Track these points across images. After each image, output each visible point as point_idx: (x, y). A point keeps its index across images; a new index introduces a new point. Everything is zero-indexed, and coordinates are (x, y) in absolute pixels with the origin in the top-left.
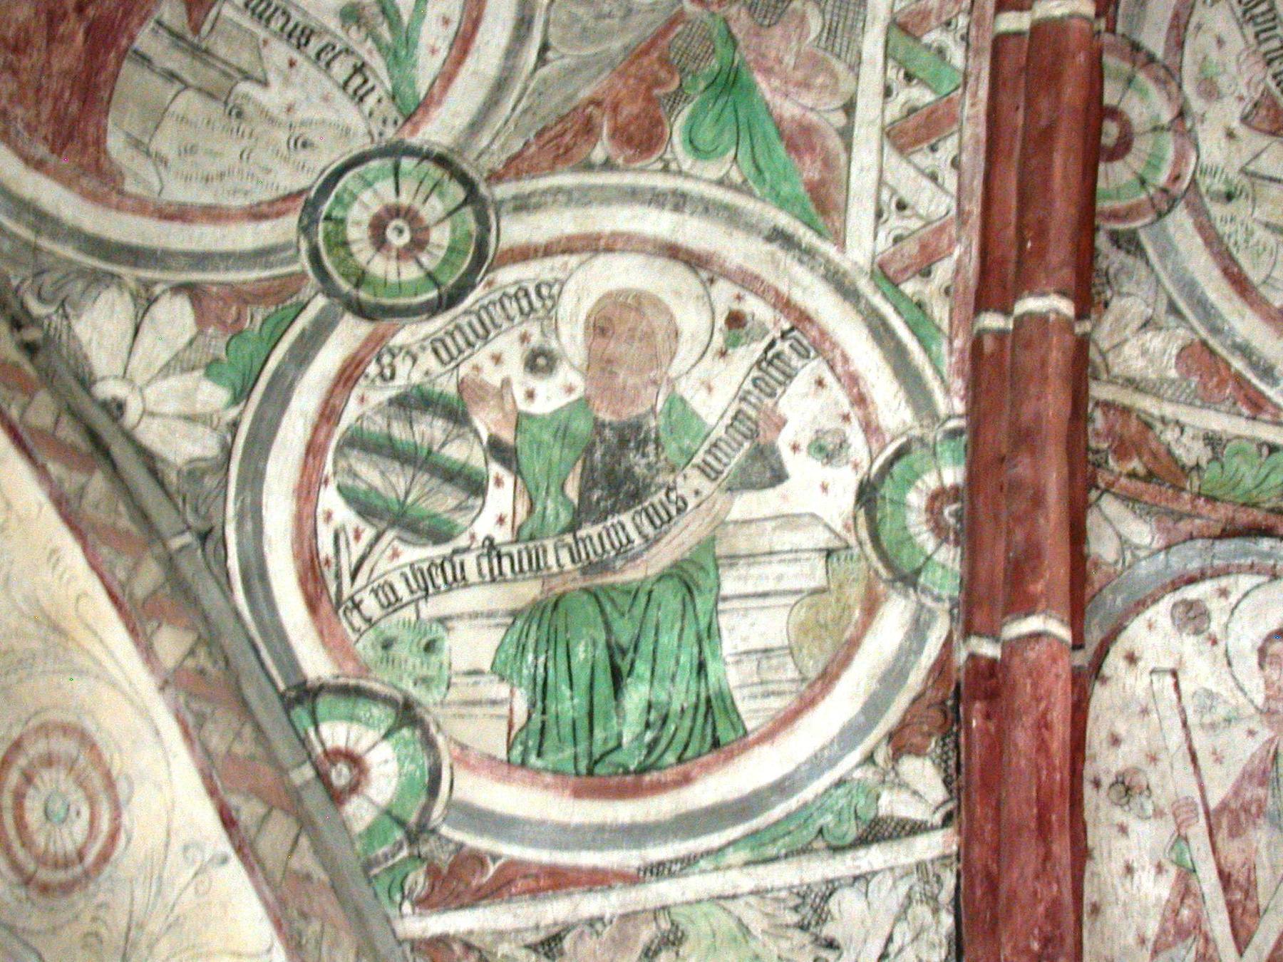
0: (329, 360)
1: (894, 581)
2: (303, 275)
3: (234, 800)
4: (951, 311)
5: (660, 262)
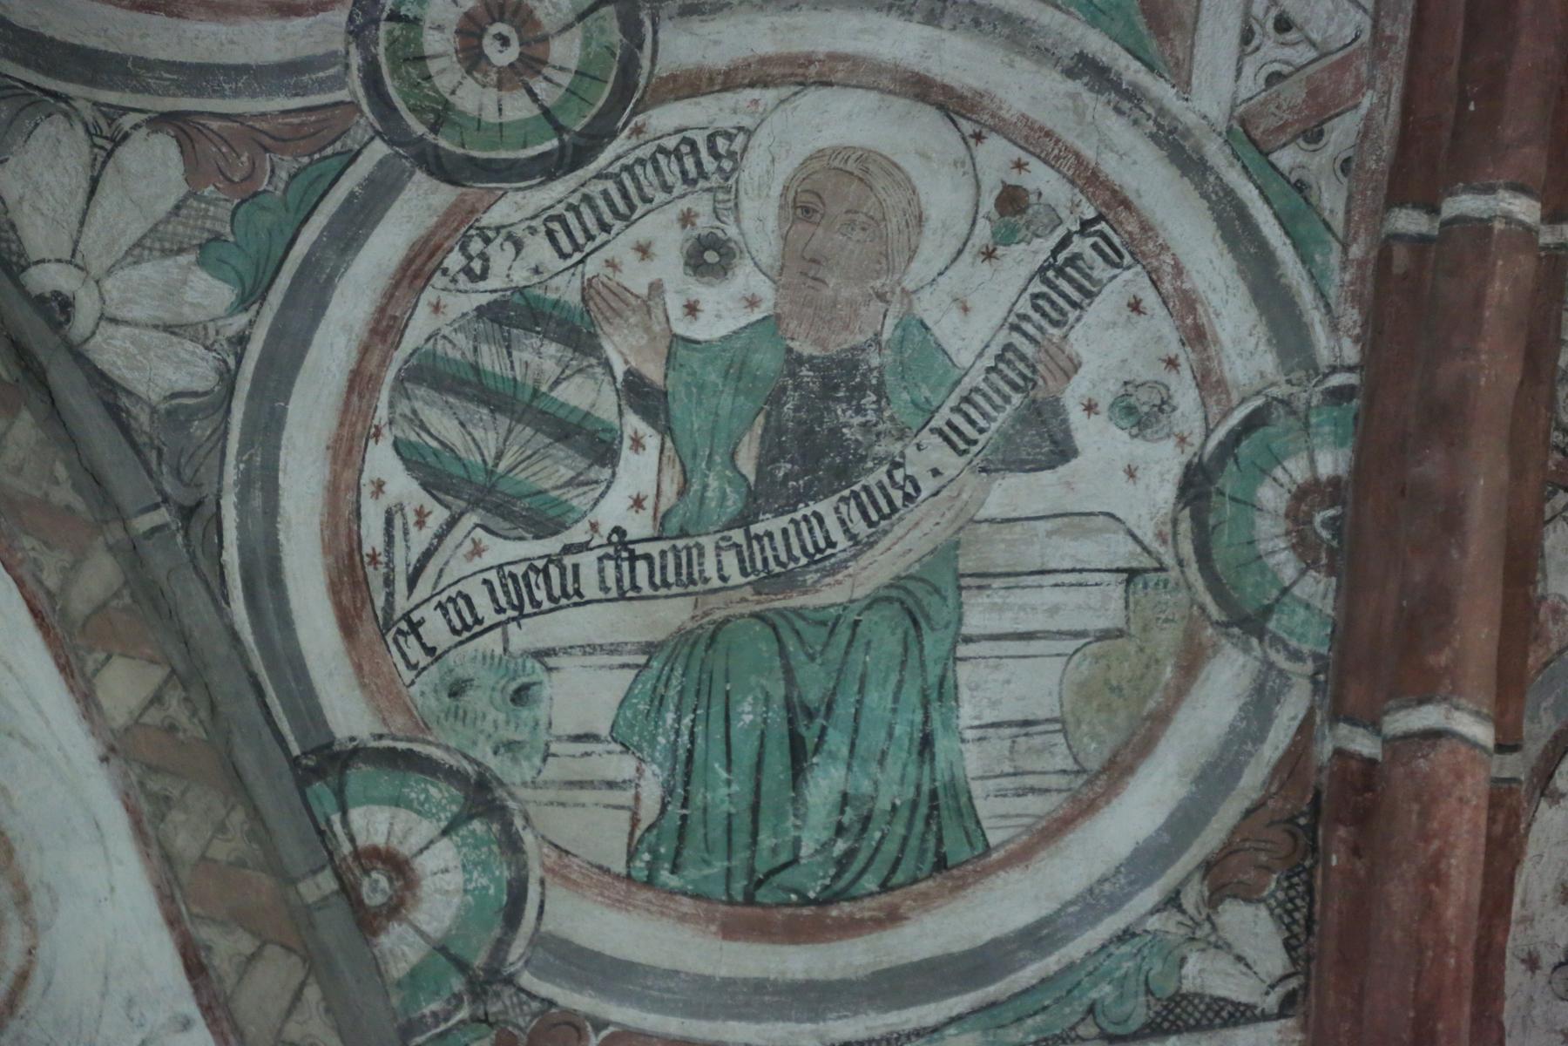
0: (387, 245)
1: (1227, 625)
2: (353, 106)
3: (205, 933)
4: (1350, 198)
5: (900, 104)
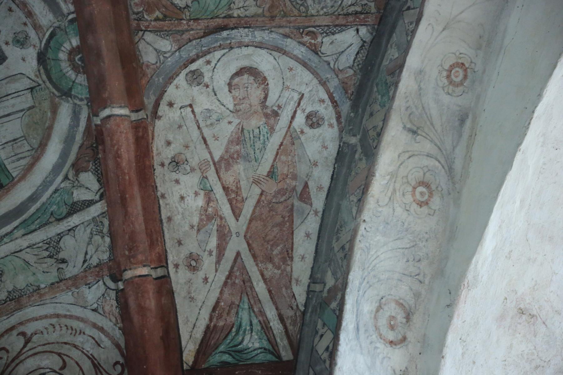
1: (61, 96)
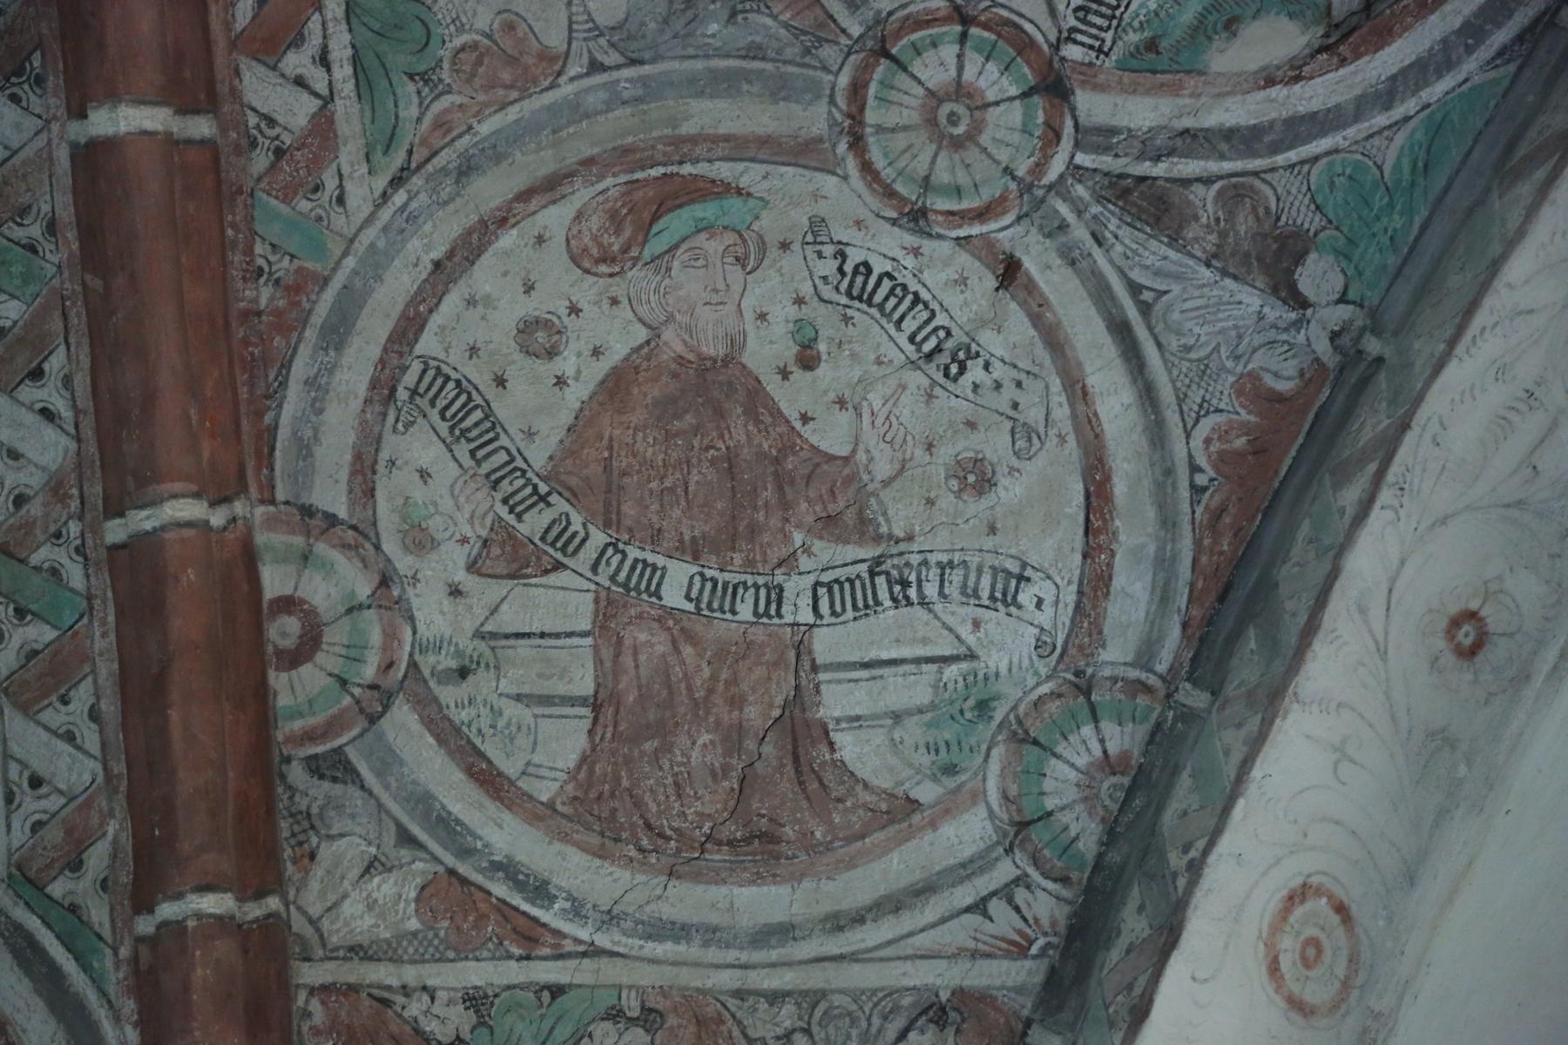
4: (112, 910)
